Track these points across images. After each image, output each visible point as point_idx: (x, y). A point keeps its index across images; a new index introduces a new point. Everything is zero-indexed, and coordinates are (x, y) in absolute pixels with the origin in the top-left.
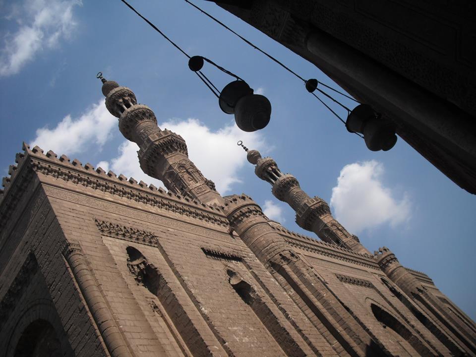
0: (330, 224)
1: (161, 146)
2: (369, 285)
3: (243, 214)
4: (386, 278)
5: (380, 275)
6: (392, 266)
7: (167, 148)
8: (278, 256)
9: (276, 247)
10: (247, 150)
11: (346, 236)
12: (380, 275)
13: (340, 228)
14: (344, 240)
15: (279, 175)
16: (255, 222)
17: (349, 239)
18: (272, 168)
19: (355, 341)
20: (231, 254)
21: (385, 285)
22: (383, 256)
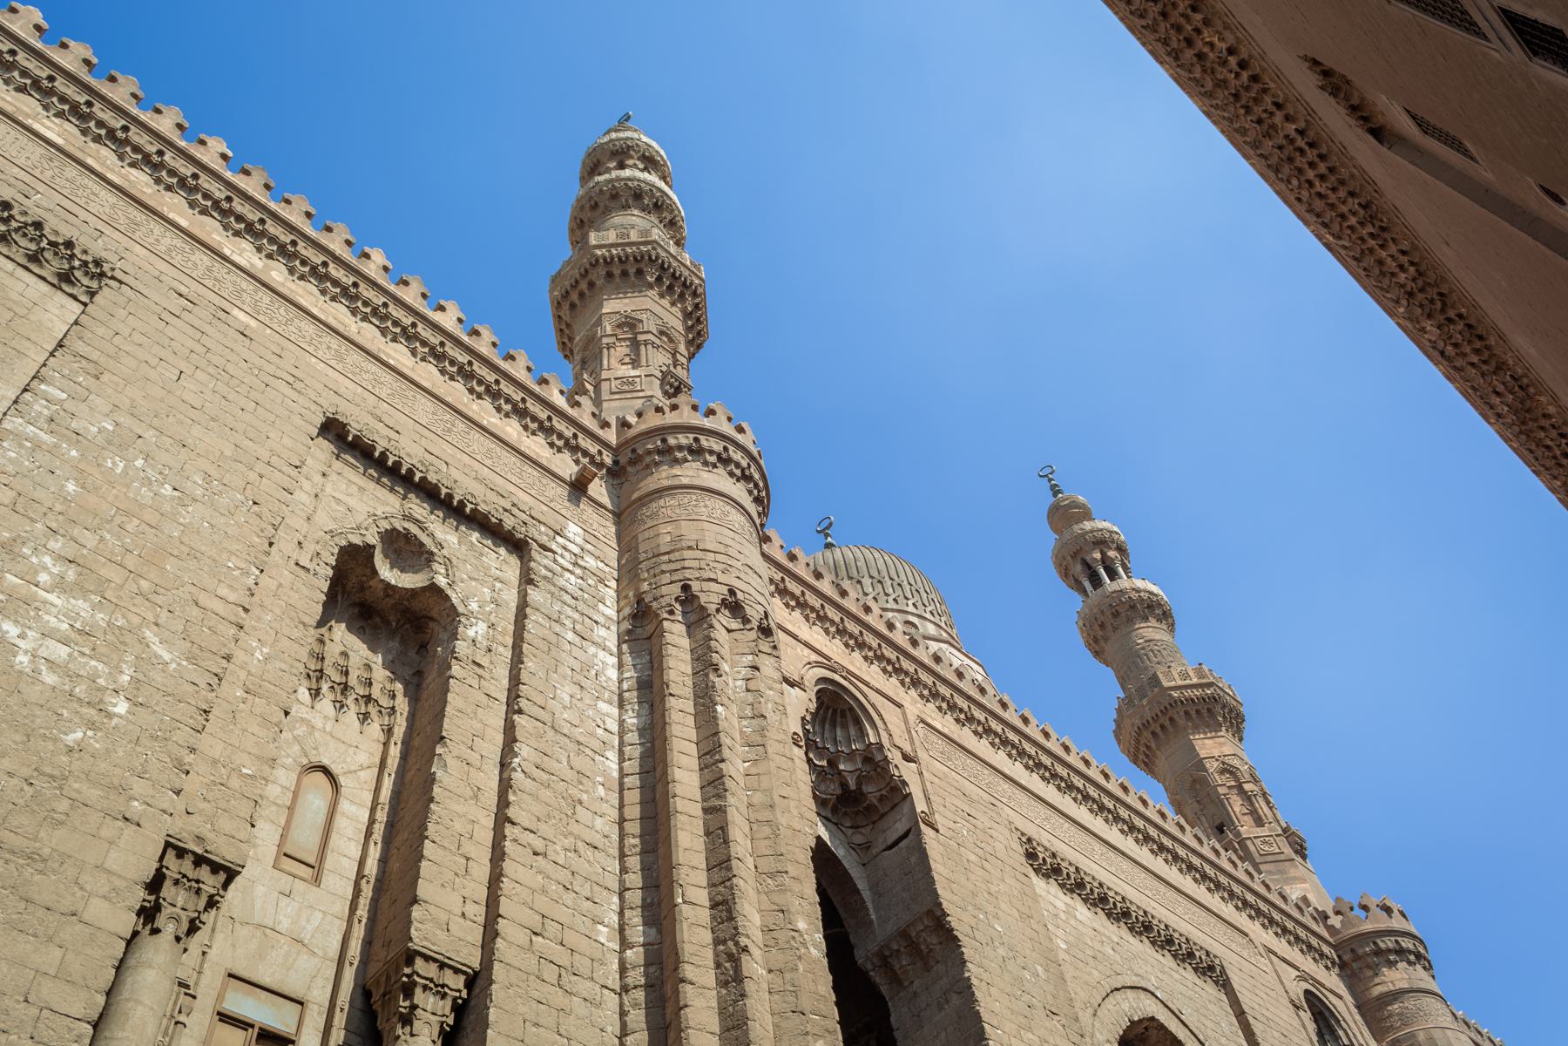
0: (1216, 764)
1: (608, 262)
2: (1211, 970)
3: (666, 451)
4: (1343, 1005)
5: (1304, 977)
6: (1396, 977)
7: (625, 274)
8: (676, 590)
9: (695, 564)
10: (1055, 491)
11: (1259, 822)
12: (1304, 977)
13: (1247, 787)
14: (1247, 828)
15: (1113, 575)
16: (685, 481)
17: (1259, 832)
18: (1103, 553)
19: (718, 965)
20: (482, 508)
21: (1306, 1016)
22: (1368, 927)
